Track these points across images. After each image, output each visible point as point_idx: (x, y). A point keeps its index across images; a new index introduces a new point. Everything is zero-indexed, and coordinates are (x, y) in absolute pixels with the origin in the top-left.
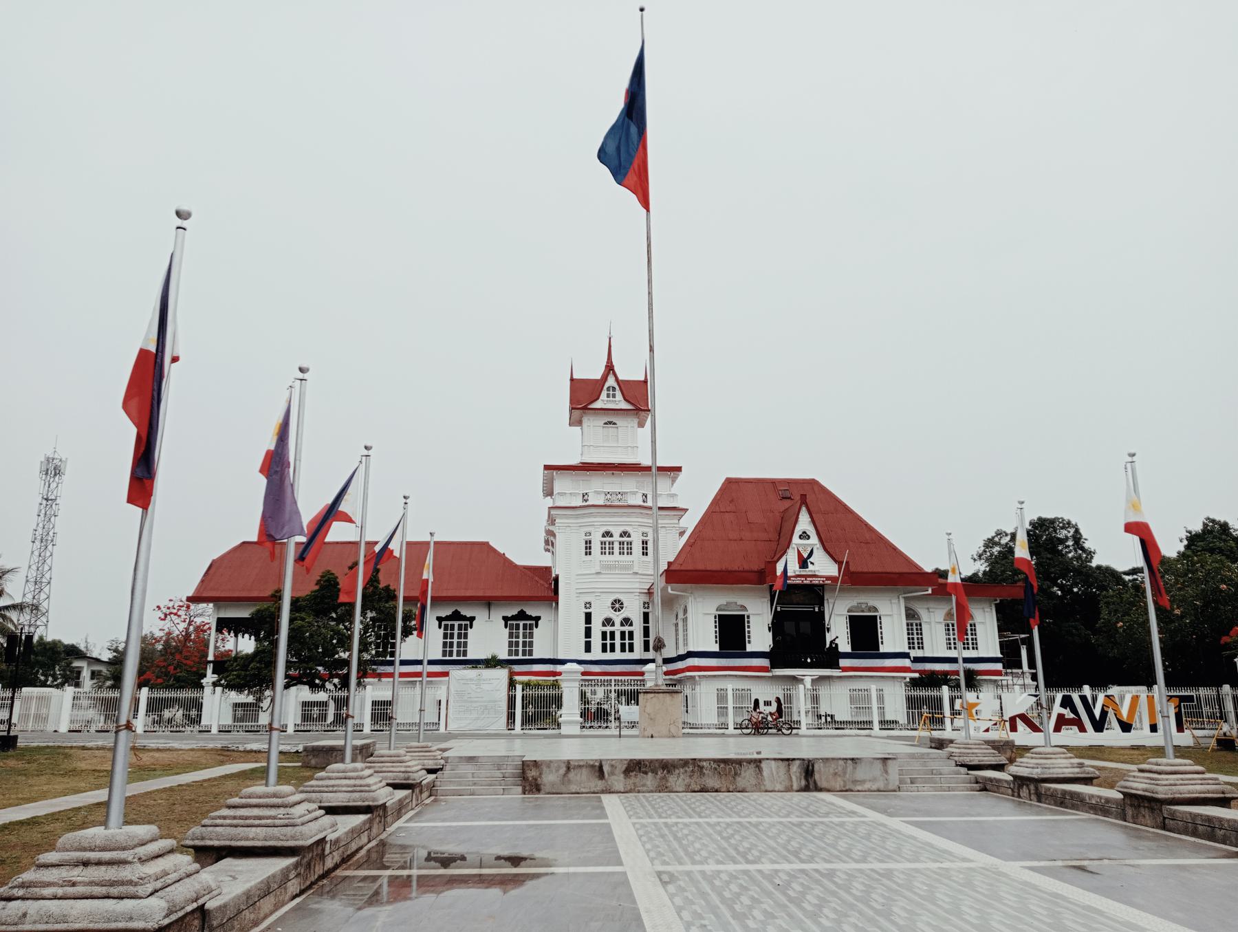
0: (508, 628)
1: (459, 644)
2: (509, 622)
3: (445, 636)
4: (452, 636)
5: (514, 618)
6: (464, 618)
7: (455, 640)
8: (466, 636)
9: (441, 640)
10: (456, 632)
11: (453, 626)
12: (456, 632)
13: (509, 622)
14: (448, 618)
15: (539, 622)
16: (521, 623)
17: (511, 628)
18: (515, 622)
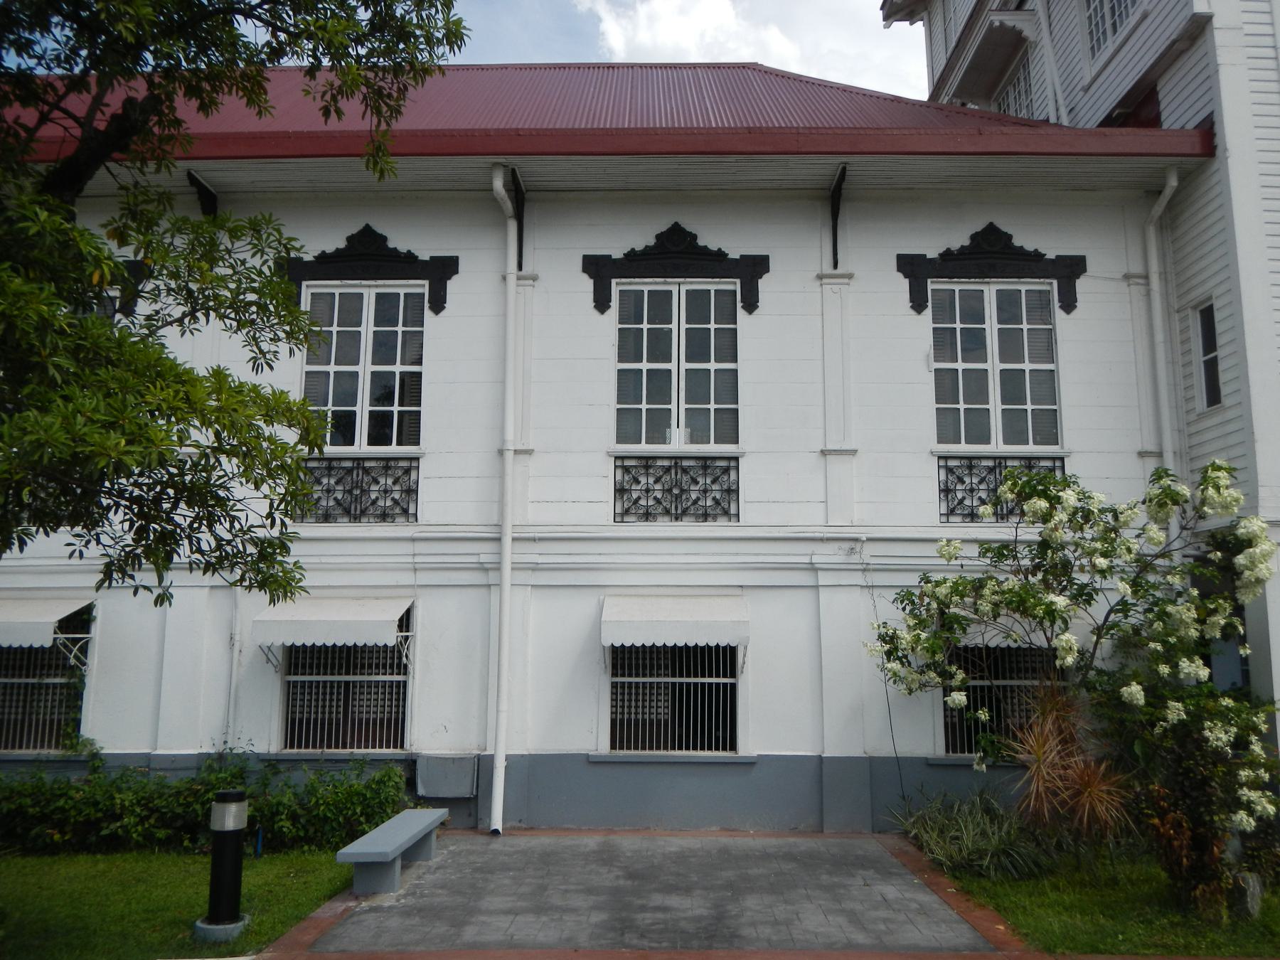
0: (928, 312)
1: (697, 383)
2: (932, 285)
3: (628, 347)
4: (660, 349)
5: (951, 264)
6: (716, 263)
7: (678, 365)
8: (729, 349)
9: (608, 365)
10: (679, 326)
11: (661, 303)
12: (679, 326)
13: (932, 285)
14: (635, 263)
15: (1082, 285)
16: (990, 291)
17: (944, 310)
18: (957, 286)
